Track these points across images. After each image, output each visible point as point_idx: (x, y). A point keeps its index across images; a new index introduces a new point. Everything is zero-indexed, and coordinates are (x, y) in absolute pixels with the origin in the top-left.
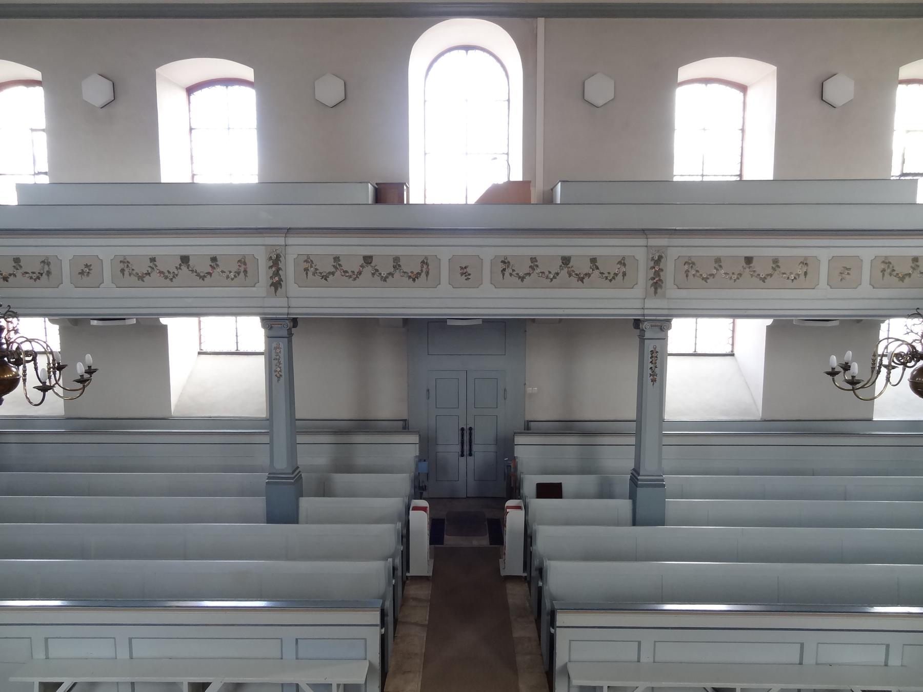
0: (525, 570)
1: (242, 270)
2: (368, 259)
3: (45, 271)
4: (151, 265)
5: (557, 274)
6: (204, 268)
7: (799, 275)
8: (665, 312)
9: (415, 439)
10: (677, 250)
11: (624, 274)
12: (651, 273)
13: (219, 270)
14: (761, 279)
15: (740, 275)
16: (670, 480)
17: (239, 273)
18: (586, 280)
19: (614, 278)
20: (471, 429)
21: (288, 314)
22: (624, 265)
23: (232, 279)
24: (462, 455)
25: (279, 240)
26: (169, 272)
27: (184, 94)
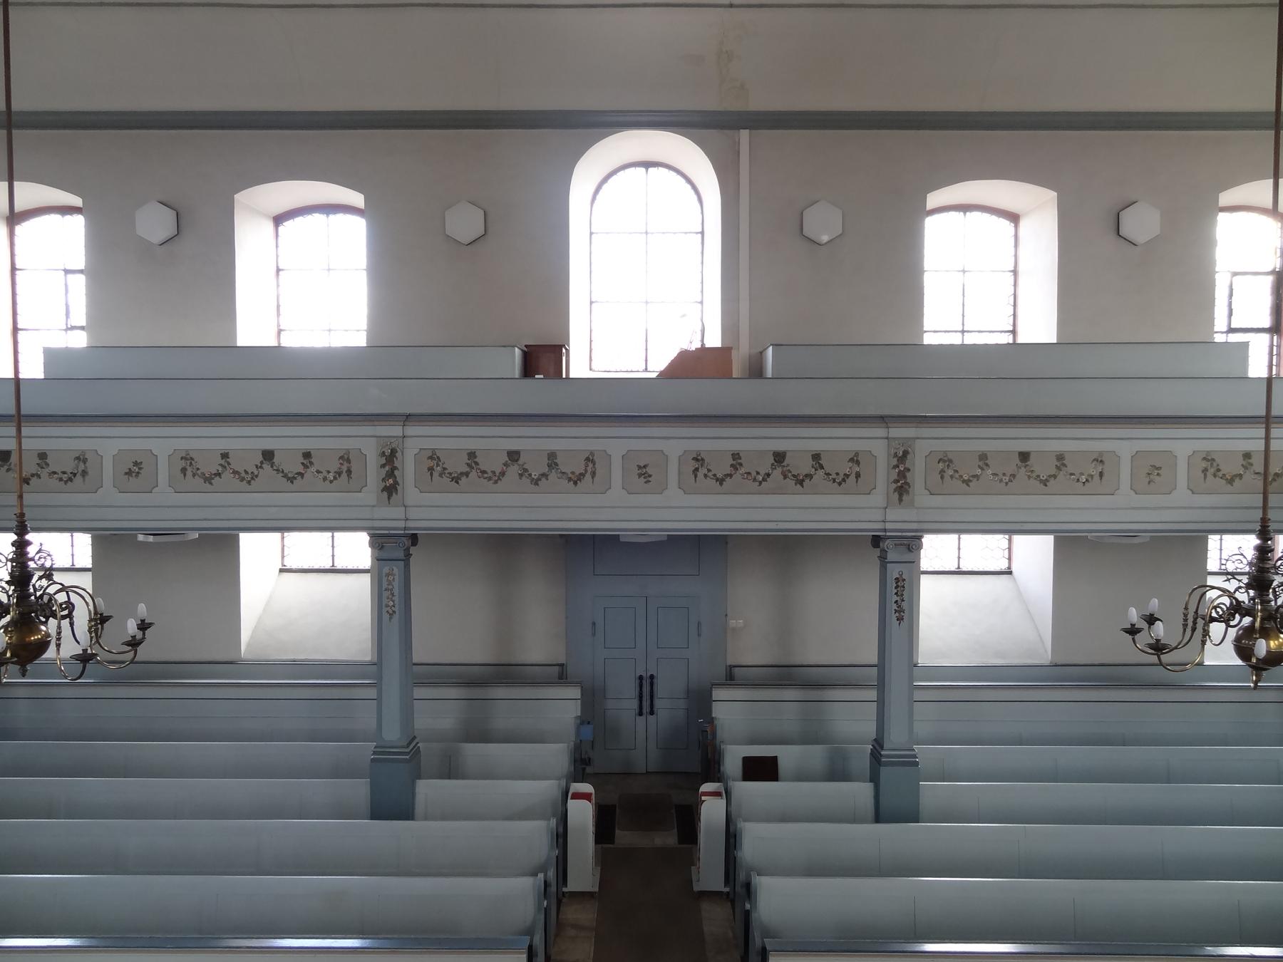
0: (727, 882)
1: (344, 468)
2: (514, 456)
3: (80, 470)
4: (223, 462)
5: (768, 475)
6: (294, 466)
7: (1092, 476)
8: (914, 526)
9: (575, 692)
10: (927, 443)
11: (858, 475)
12: (894, 475)
13: (313, 469)
14: (1041, 481)
15: (1014, 476)
16: (926, 753)
17: (340, 474)
18: (807, 481)
19: (844, 480)
20: (652, 677)
21: (405, 529)
22: (858, 463)
24: (641, 714)
25: (396, 430)
26: (246, 472)
27: (270, 226)
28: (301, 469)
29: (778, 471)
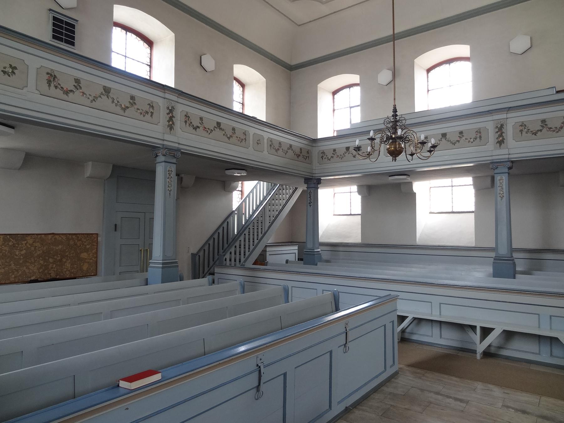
1: (478, 136)
13: (464, 138)
17: (476, 138)
21: (508, 158)
23: (472, 142)
25: (504, 116)
28: (458, 139)
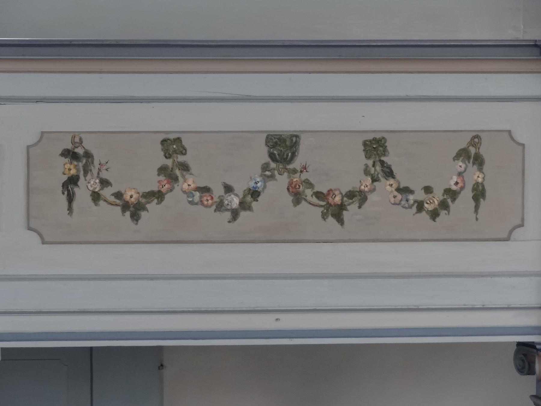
5: (255, 194)
11: (479, 193)
18: (352, 212)
19: (444, 205)
22: (479, 161)
29: (277, 189)
